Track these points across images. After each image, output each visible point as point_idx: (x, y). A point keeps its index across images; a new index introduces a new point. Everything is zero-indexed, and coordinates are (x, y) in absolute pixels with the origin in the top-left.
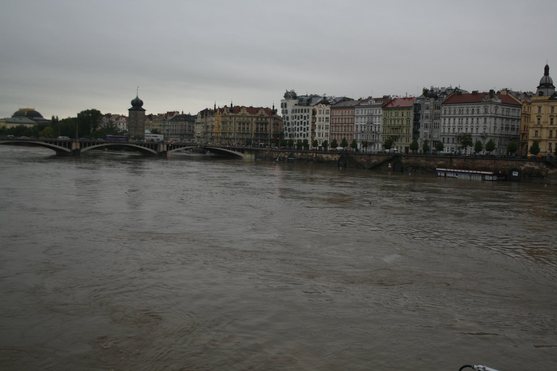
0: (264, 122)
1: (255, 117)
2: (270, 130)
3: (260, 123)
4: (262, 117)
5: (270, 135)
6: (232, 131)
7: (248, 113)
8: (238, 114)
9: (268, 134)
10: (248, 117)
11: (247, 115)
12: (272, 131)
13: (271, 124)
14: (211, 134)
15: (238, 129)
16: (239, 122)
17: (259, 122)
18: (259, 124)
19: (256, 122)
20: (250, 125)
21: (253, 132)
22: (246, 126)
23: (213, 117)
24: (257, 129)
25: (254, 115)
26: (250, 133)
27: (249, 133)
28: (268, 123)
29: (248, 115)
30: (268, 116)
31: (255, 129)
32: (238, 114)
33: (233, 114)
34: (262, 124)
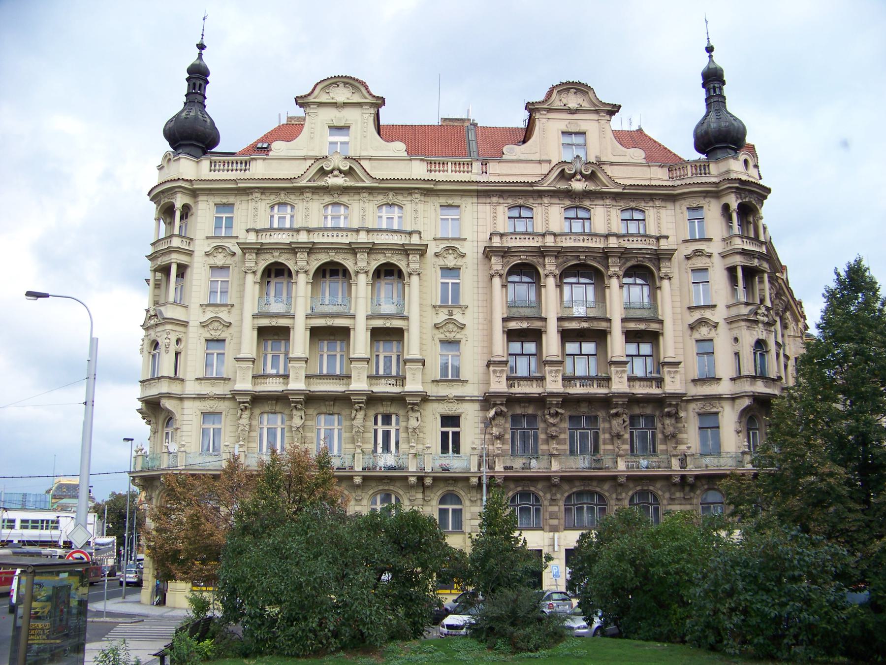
0: (613, 242)
1: (485, 193)
3: (559, 253)
4: (578, 185)
7: (398, 148)
15: (249, 344)
16: (259, 250)
17: (542, 252)
18: (550, 266)
19: (505, 253)
21: (473, 390)
25: (475, 173)
26: (425, 399)
27: (399, 400)
28: (661, 256)
29: (381, 172)
32: (259, 169)
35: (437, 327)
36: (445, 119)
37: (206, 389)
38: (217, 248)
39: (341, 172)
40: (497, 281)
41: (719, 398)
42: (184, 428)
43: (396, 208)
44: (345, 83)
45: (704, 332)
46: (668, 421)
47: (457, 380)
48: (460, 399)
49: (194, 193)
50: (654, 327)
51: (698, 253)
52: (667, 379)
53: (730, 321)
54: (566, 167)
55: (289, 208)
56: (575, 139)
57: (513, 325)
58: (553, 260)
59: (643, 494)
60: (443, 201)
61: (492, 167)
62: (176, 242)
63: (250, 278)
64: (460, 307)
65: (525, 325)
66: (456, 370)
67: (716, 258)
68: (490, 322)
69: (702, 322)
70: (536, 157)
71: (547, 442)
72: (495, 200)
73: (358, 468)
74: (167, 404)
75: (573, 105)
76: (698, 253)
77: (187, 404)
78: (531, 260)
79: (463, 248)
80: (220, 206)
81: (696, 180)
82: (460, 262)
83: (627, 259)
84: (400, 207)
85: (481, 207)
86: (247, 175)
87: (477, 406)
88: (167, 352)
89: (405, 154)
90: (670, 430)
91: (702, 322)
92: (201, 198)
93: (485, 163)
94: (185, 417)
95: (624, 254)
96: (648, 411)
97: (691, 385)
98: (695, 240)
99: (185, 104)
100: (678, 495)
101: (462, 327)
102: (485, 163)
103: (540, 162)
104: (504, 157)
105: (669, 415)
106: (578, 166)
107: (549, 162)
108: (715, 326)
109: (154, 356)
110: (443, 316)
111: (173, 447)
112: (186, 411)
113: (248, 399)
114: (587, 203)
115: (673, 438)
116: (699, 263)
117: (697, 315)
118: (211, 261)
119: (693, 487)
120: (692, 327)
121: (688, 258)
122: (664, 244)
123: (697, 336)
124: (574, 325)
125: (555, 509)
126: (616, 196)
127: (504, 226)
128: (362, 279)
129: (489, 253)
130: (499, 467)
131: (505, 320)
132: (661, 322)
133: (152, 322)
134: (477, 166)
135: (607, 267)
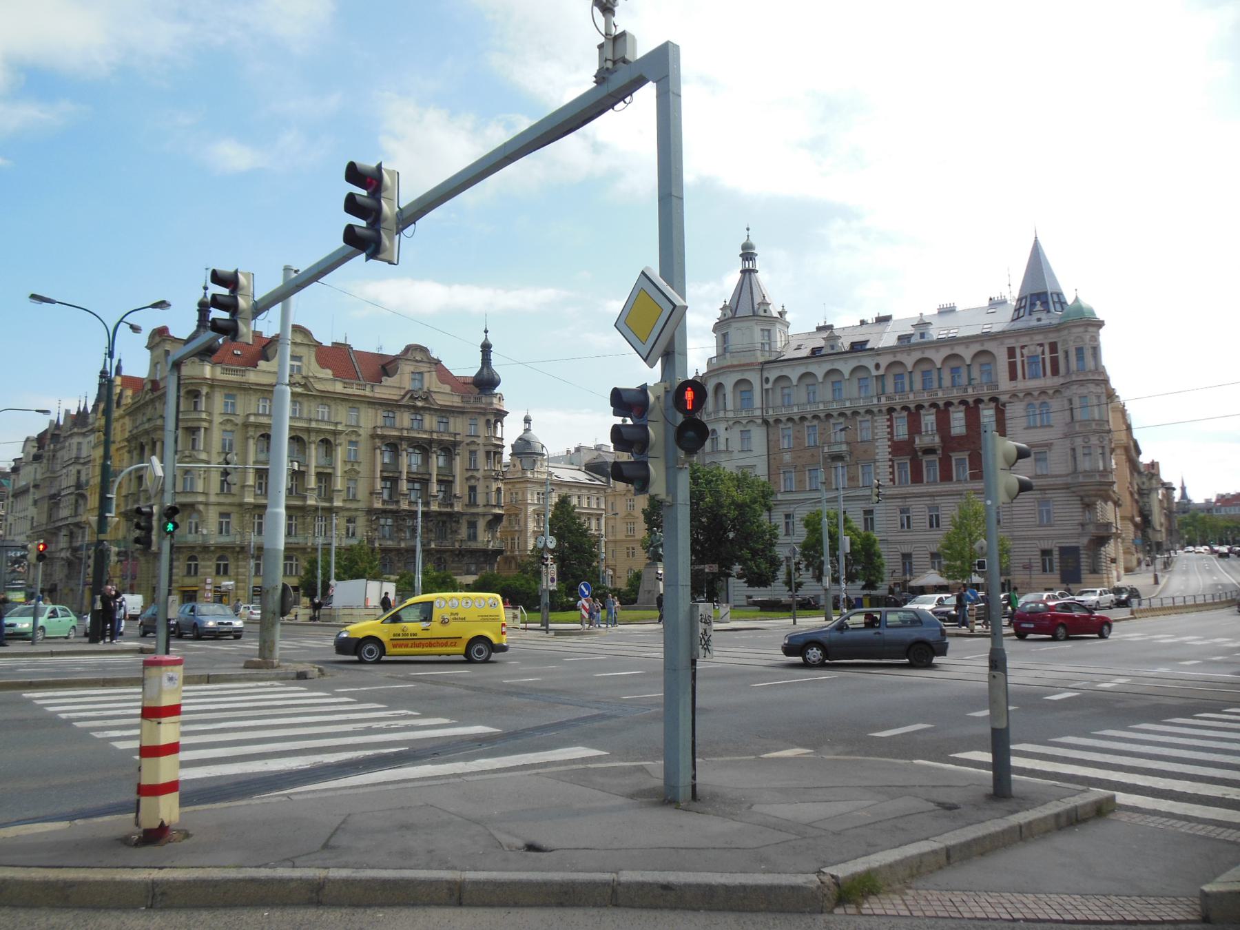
0: (435, 436)
1: (374, 403)
2: (473, 489)
4: (420, 404)
5: (472, 525)
6: (205, 494)
7: (328, 373)
8: (252, 377)
9: (453, 517)
10: (326, 398)
11: (319, 386)
12: (481, 499)
13: (473, 453)
14: (72, 535)
17: (401, 438)
19: (383, 437)
20: (340, 453)
21: (361, 505)
22: (314, 456)
23: (84, 434)
24: (392, 480)
28: (455, 444)
30: (456, 401)
31: (379, 485)
32: (252, 377)
33: (219, 374)
34: (423, 448)
35: (345, 472)
36: (335, 343)
37: (222, 499)
38: (228, 420)
39: (300, 385)
40: (378, 452)
41: (478, 514)
42: (210, 521)
43: (327, 408)
44: (301, 331)
45: (473, 482)
46: (454, 524)
47: (354, 500)
48: (357, 510)
49: (212, 386)
50: (451, 479)
51: (473, 443)
52: (455, 505)
53: (486, 478)
54: (414, 393)
55: (268, 401)
56: (417, 376)
57: (385, 474)
58: (406, 443)
59: (440, 559)
60: (350, 405)
61: (377, 389)
62: (204, 416)
63: (251, 442)
64: (357, 462)
65: (391, 475)
66: (354, 495)
67: (481, 447)
68: (374, 471)
69: (472, 477)
70: (398, 385)
71: (397, 532)
72: (377, 406)
73: (309, 544)
74: (201, 507)
75: (418, 358)
76: (473, 443)
77: (211, 508)
78: (398, 441)
79: (361, 432)
80: (227, 396)
81: (476, 406)
82: (358, 439)
83: (441, 444)
84: (329, 406)
85: (370, 410)
86: (243, 379)
87: (364, 514)
88: (200, 478)
89: (332, 377)
90: (454, 529)
91: (472, 477)
92: (216, 389)
93: (372, 386)
94: (210, 515)
95: (440, 442)
96: (445, 518)
97: (465, 508)
98: (472, 436)
99: (199, 326)
100: (456, 559)
101: (358, 473)
102: (372, 386)
103: (400, 388)
104: (382, 384)
105: (455, 522)
106: (420, 393)
107: (404, 388)
108: (478, 479)
109: (184, 479)
110: (349, 467)
111: (205, 532)
112: (210, 511)
113: (252, 507)
114: (422, 412)
115: (455, 532)
116: (473, 448)
117: (470, 474)
118: (223, 427)
119: (463, 556)
120: (468, 479)
121: (468, 444)
122: (458, 438)
123: (469, 484)
124: (414, 476)
125: (400, 565)
126: (436, 410)
127: (380, 422)
128: (313, 446)
129: (374, 436)
130: (377, 545)
131: (381, 471)
132: (454, 476)
133: (187, 460)
134: (368, 388)
135: (431, 447)
